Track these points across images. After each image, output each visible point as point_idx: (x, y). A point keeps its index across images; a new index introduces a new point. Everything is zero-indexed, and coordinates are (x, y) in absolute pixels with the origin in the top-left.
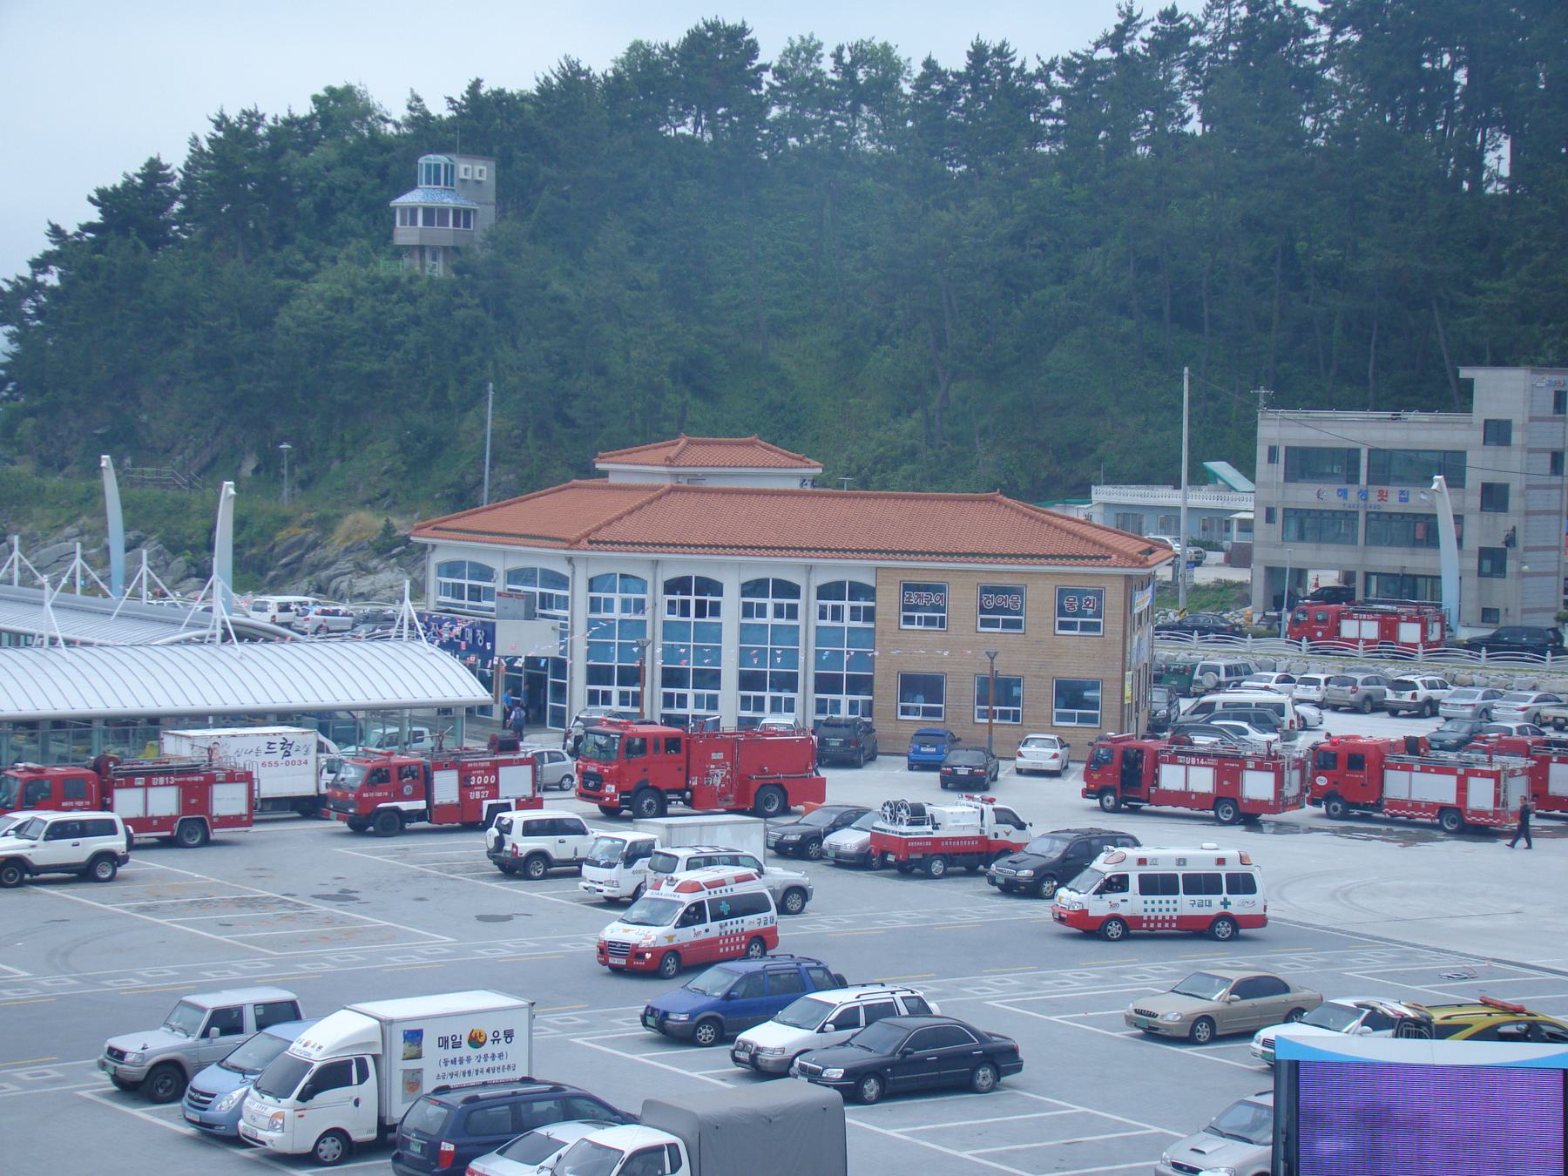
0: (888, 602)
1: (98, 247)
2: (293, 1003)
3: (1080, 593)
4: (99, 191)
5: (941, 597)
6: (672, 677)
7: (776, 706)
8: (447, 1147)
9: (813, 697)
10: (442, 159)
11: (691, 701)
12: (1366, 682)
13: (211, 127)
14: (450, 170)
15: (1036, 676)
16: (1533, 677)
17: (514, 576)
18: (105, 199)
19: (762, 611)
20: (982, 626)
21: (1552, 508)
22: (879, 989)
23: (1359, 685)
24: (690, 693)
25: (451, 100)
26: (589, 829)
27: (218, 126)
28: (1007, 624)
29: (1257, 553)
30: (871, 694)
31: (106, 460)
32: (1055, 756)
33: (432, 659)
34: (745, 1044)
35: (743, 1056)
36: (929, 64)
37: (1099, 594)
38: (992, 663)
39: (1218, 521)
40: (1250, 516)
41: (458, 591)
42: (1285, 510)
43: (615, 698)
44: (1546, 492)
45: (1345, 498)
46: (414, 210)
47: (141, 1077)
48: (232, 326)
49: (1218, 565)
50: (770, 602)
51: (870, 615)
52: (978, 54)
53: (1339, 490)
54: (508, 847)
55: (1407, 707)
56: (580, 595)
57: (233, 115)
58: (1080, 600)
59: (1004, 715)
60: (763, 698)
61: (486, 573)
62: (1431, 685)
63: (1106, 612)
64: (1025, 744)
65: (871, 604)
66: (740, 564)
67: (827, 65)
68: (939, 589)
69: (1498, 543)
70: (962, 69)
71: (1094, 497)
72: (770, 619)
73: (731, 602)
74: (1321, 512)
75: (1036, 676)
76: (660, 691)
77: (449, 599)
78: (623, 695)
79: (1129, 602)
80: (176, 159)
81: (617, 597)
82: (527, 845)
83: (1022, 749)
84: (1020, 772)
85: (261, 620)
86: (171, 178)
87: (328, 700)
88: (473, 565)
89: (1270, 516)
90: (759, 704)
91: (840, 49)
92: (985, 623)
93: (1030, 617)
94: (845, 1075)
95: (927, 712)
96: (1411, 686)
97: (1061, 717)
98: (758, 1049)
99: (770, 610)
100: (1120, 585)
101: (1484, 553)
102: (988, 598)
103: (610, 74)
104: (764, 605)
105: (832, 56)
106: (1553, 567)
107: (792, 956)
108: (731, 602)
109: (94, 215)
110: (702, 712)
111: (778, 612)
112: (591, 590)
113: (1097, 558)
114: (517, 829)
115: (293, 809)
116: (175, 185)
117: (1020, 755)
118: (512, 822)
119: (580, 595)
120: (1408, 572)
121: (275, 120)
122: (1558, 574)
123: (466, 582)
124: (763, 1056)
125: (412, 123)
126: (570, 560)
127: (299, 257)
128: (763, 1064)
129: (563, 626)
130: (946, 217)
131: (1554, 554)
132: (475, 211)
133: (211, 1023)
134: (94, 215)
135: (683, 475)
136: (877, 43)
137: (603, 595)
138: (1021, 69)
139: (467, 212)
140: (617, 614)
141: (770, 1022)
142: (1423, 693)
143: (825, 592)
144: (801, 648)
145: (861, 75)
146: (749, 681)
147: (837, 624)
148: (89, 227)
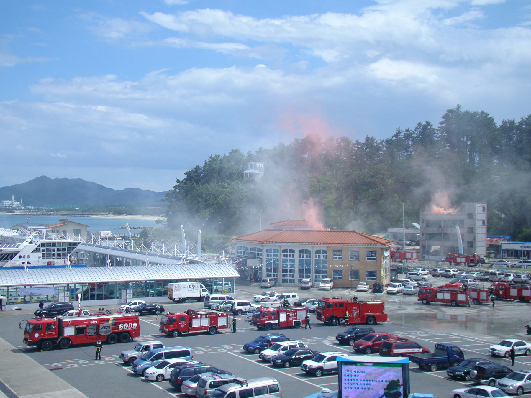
0: (330, 254)
1: (186, 183)
2: (161, 345)
3: (371, 252)
4: (186, 172)
6: (285, 271)
7: (306, 277)
8: (179, 378)
9: (314, 275)
10: (253, 163)
11: (288, 276)
12: (440, 270)
13: (209, 158)
14: (255, 165)
16: (477, 269)
17: (251, 249)
18: (188, 174)
19: (303, 257)
22: (294, 341)
23: (439, 271)
24: (288, 274)
25: (256, 151)
26: (251, 304)
27: (210, 158)
29: (420, 243)
30: (327, 274)
31: (182, 227)
32: (365, 287)
33: (228, 268)
34: (262, 354)
35: (261, 357)
36: (357, 141)
37: (375, 252)
39: (414, 235)
40: (419, 235)
41: (241, 253)
43: (272, 275)
46: (247, 174)
47: (127, 360)
48: (210, 198)
49: (414, 245)
50: (305, 254)
51: (326, 257)
52: (367, 139)
54: (234, 308)
55: (449, 275)
56: (265, 253)
57: (213, 156)
59: (356, 278)
60: (303, 275)
61: (247, 249)
62: (454, 271)
63: (377, 256)
64: (359, 284)
65: (326, 254)
66: (298, 246)
67: (335, 142)
69: (471, 240)
70: (364, 142)
71: (388, 231)
73: (297, 254)
74: (434, 233)
76: (282, 274)
77: (239, 254)
78: (274, 275)
79: (382, 254)
80: (202, 165)
81: (272, 254)
82: (237, 308)
83: (358, 286)
84: (358, 291)
85: (196, 259)
86: (201, 169)
87: (204, 277)
88: (244, 247)
89: (423, 234)
90: (303, 277)
91: (338, 139)
94: (281, 362)
95: (339, 278)
96: (449, 271)
97: (368, 279)
98: (265, 355)
99: (305, 256)
101: (468, 242)
103: (289, 145)
104: (304, 255)
105: (336, 140)
106: (484, 245)
107: (278, 334)
108: (297, 254)
109: (186, 177)
110: (291, 278)
111: (307, 256)
112: (267, 252)
113: (375, 244)
114: (236, 304)
115: (195, 300)
116: (202, 170)
117: (358, 287)
118: (234, 303)
119: (265, 253)
121: (222, 157)
122: (485, 247)
123: (243, 251)
124: (265, 357)
125: (249, 156)
126: (262, 246)
127: (226, 184)
128: (265, 358)
129: (261, 260)
130: (357, 172)
131: (484, 242)
132: (260, 174)
133: (143, 348)
134: (186, 177)
135: (288, 227)
136: (345, 137)
137: (269, 253)
138: (376, 142)
139: (258, 174)
140: (272, 257)
141: (268, 349)
142: (452, 273)
143: (318, 252)
144: (312, 264)
145: (342, 144)
146: (301, 271)
148: (185, 179)
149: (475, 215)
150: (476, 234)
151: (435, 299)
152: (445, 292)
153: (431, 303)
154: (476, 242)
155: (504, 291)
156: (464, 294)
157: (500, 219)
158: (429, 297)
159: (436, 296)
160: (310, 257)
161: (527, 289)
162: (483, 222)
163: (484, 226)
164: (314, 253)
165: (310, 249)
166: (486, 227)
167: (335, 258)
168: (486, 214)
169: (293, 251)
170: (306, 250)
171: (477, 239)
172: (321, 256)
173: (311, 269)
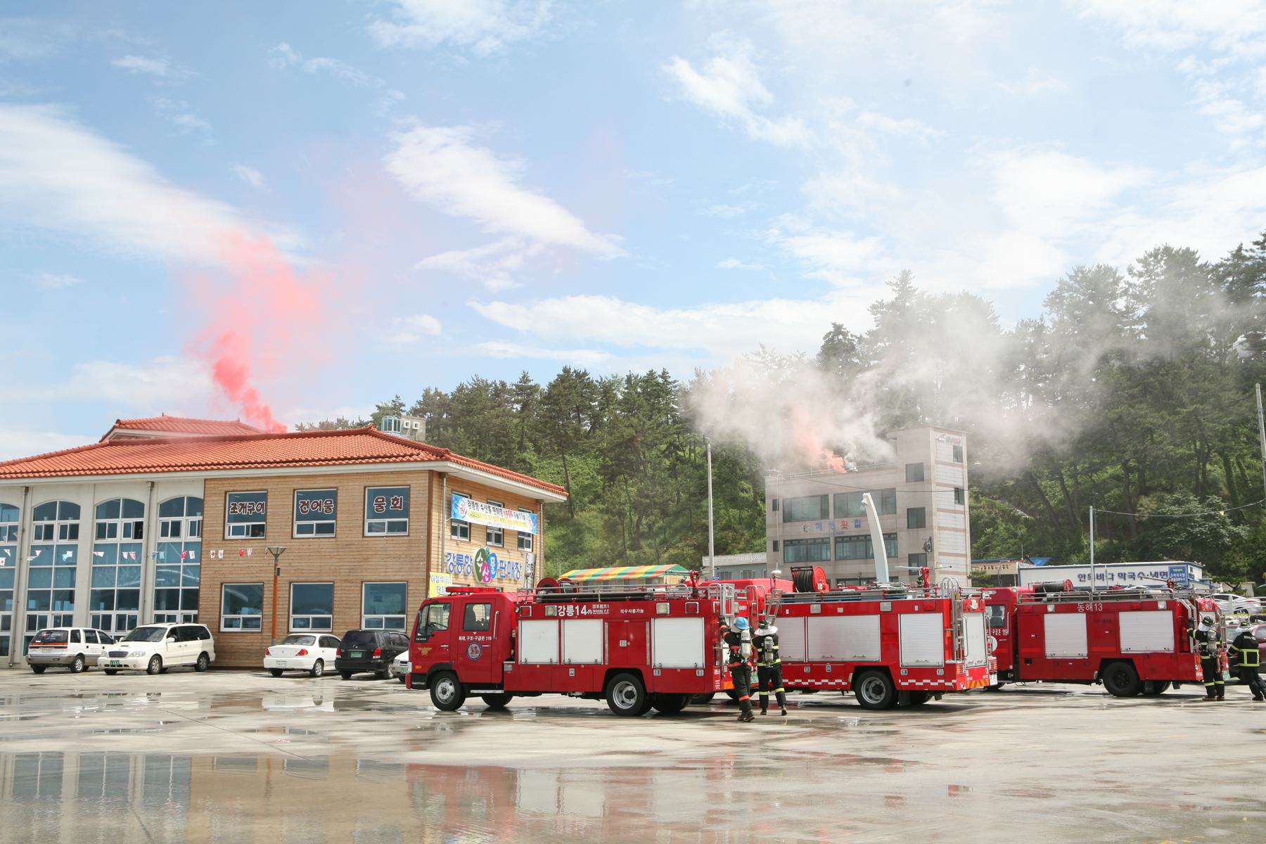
3: (389, 493)
5: (262, 505)
15: (346, 581)
20: (299, 532)
21: (958, 527)
28: (322, 529)
37: (406, 493)
38: (276, 560)
42: (784, 541)
44: (953, 515)
45: (821, 529)
53: (817, 524)
58: (388, 501)
60: (110, 616)
68: (262, 497)
72: (120, 539)
73: (87, 522)
75: (346, 581)
92: (302, 529)
93: (341, 522)
100: (425, 481)
102: (304, 503)
104: (116, 525)
117: (268, 653)
120: (863, 576)
143: (171, 507)
147: (175, 540)
149: (929, 468)
150: (935, 531)
151: (508, 667)
152: (570, 609)
153: (472, 691)
154: (936, 554)
155: (1006, 632)
156: (691, 614)
157: (1015, 520)
158: (474, 653)
159: (513, 643)
160: (138, 534)
161: (1152, 606)
162: (958, 493)
163: (960, 507)
164: (155, 510)
165: (139, 496)
166: (967, 509)
167: (237, 531)
168: (966, 471)
169: (71, 510)
170: (127, 501)
171: (938, 547)
172: (185, 529)
173: (141, 588)
